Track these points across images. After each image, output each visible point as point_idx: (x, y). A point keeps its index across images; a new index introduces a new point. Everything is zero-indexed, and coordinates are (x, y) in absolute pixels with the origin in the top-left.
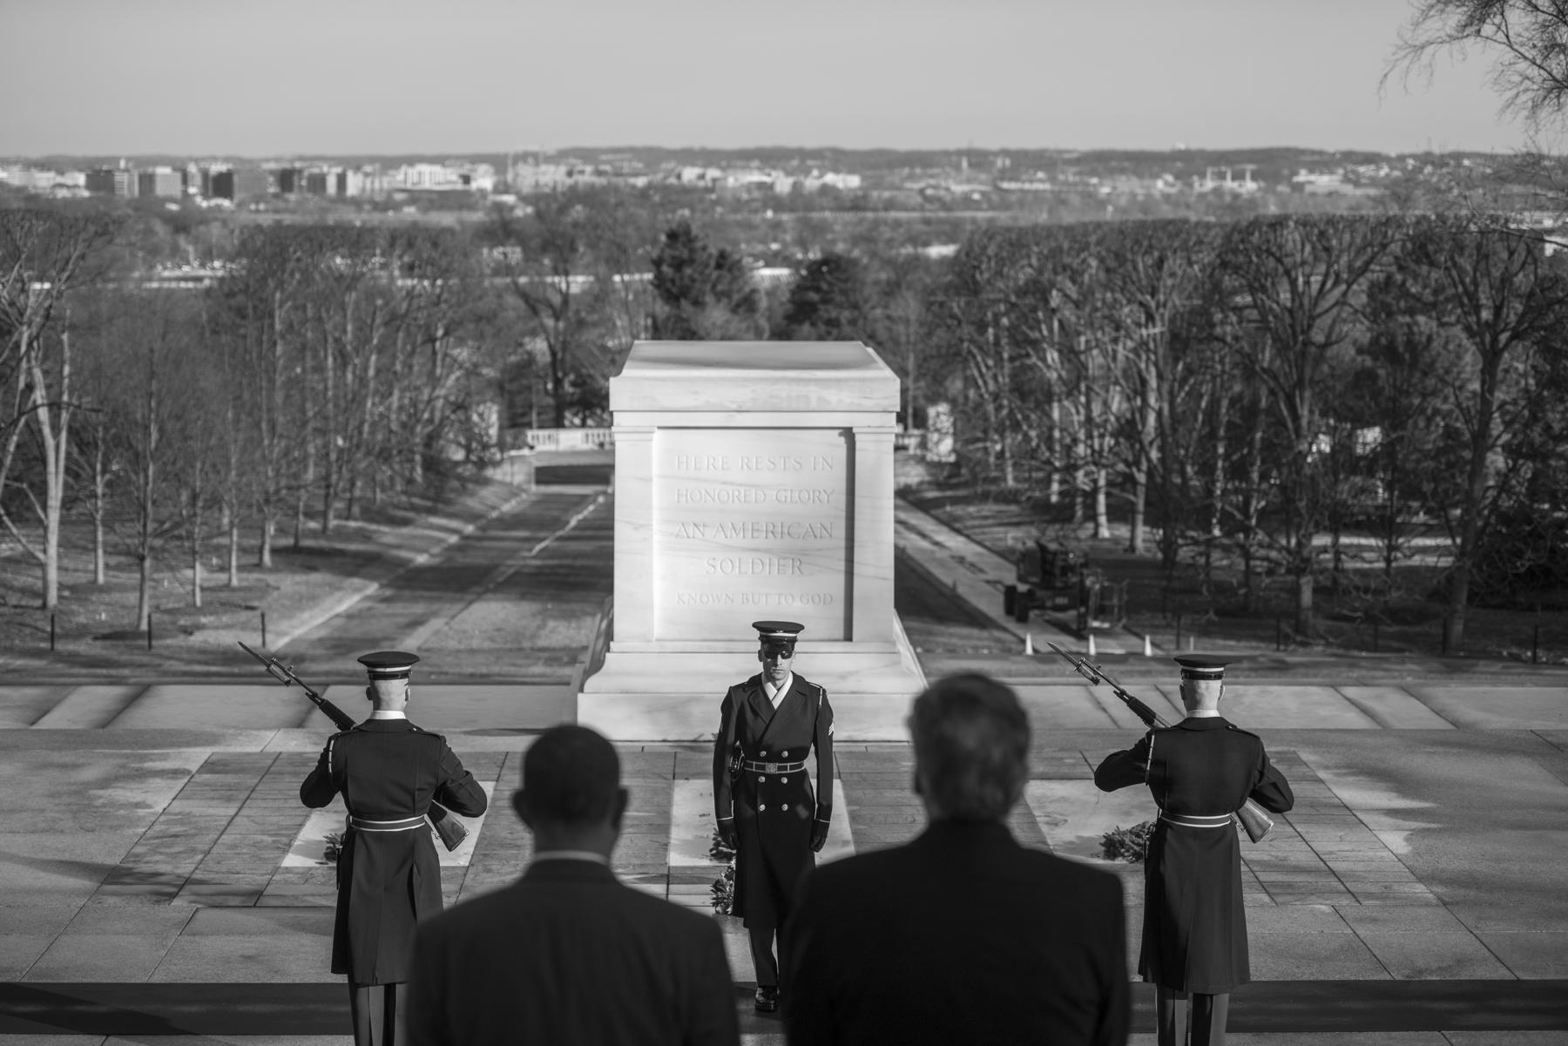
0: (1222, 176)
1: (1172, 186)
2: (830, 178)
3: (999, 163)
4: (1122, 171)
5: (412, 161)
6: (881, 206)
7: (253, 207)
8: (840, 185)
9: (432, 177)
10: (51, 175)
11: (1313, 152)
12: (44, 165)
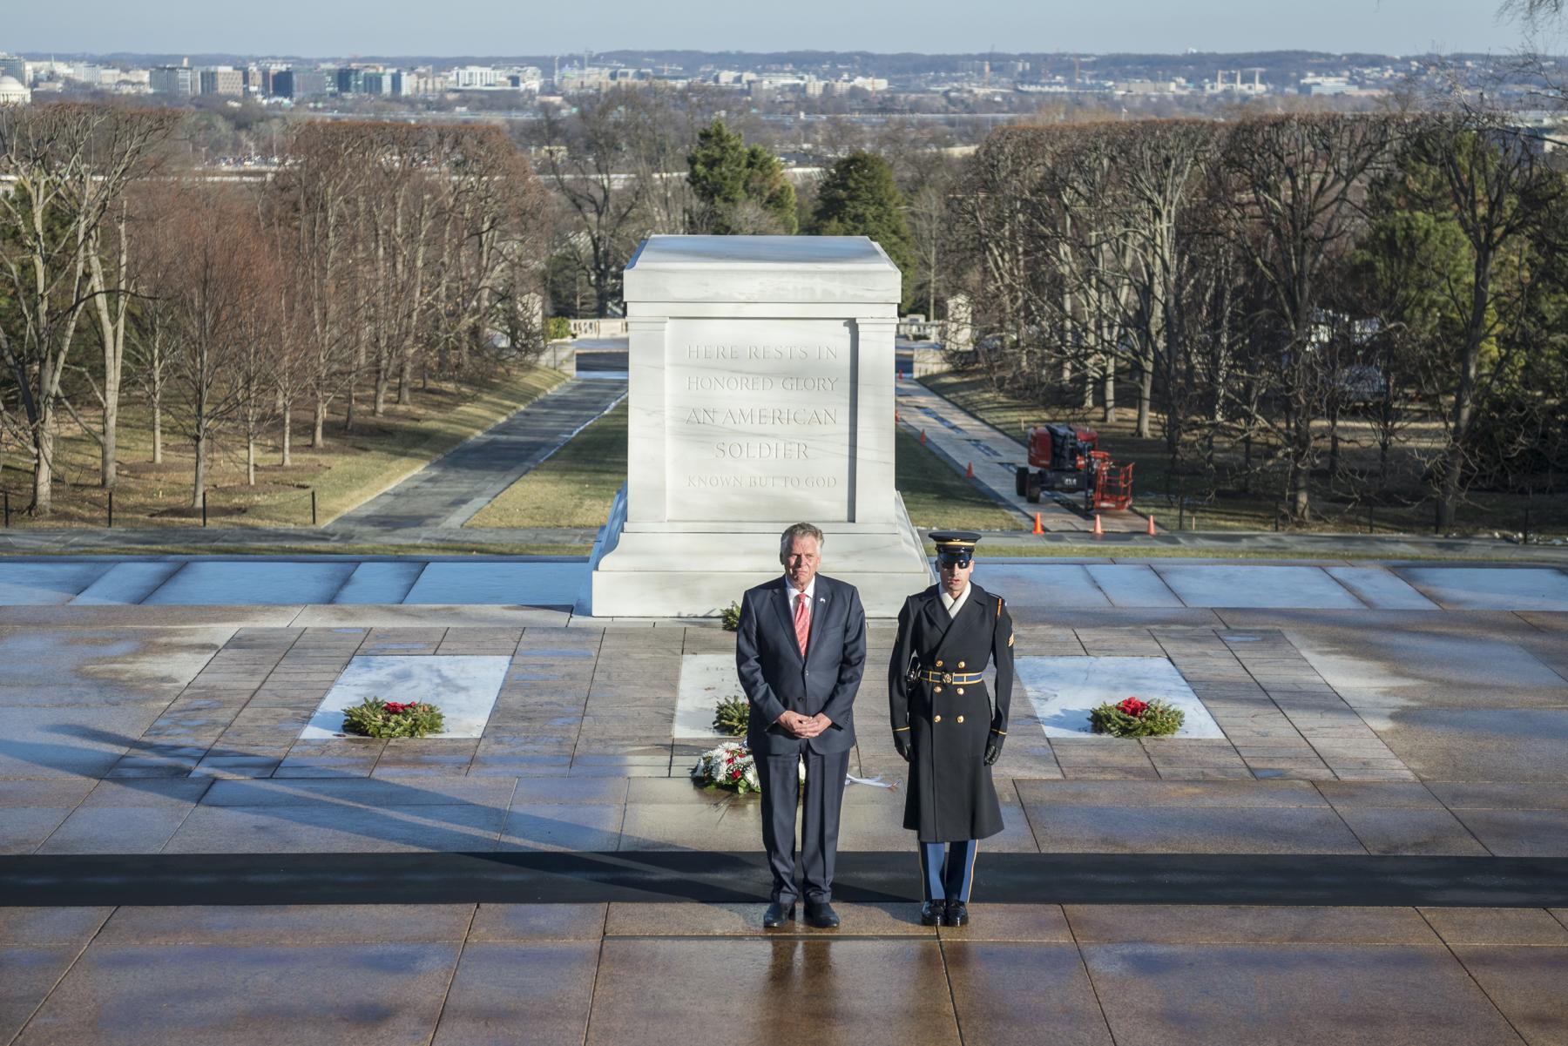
0: (1232, 79)
1: (1184, 88)
2: (859, 81)
3: (1020, 67)
4: (1137, 74)
5: (463, 62)
6: (907, 107)
7: (311, 105)
8: (869, 88)
9: (481, 78)
10: (117, 71)
11: (1320, 55)
12: (108, 62)
